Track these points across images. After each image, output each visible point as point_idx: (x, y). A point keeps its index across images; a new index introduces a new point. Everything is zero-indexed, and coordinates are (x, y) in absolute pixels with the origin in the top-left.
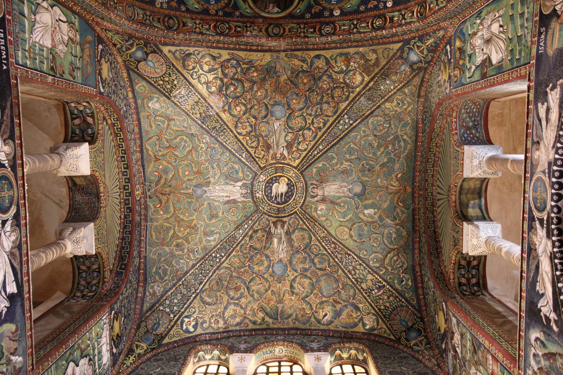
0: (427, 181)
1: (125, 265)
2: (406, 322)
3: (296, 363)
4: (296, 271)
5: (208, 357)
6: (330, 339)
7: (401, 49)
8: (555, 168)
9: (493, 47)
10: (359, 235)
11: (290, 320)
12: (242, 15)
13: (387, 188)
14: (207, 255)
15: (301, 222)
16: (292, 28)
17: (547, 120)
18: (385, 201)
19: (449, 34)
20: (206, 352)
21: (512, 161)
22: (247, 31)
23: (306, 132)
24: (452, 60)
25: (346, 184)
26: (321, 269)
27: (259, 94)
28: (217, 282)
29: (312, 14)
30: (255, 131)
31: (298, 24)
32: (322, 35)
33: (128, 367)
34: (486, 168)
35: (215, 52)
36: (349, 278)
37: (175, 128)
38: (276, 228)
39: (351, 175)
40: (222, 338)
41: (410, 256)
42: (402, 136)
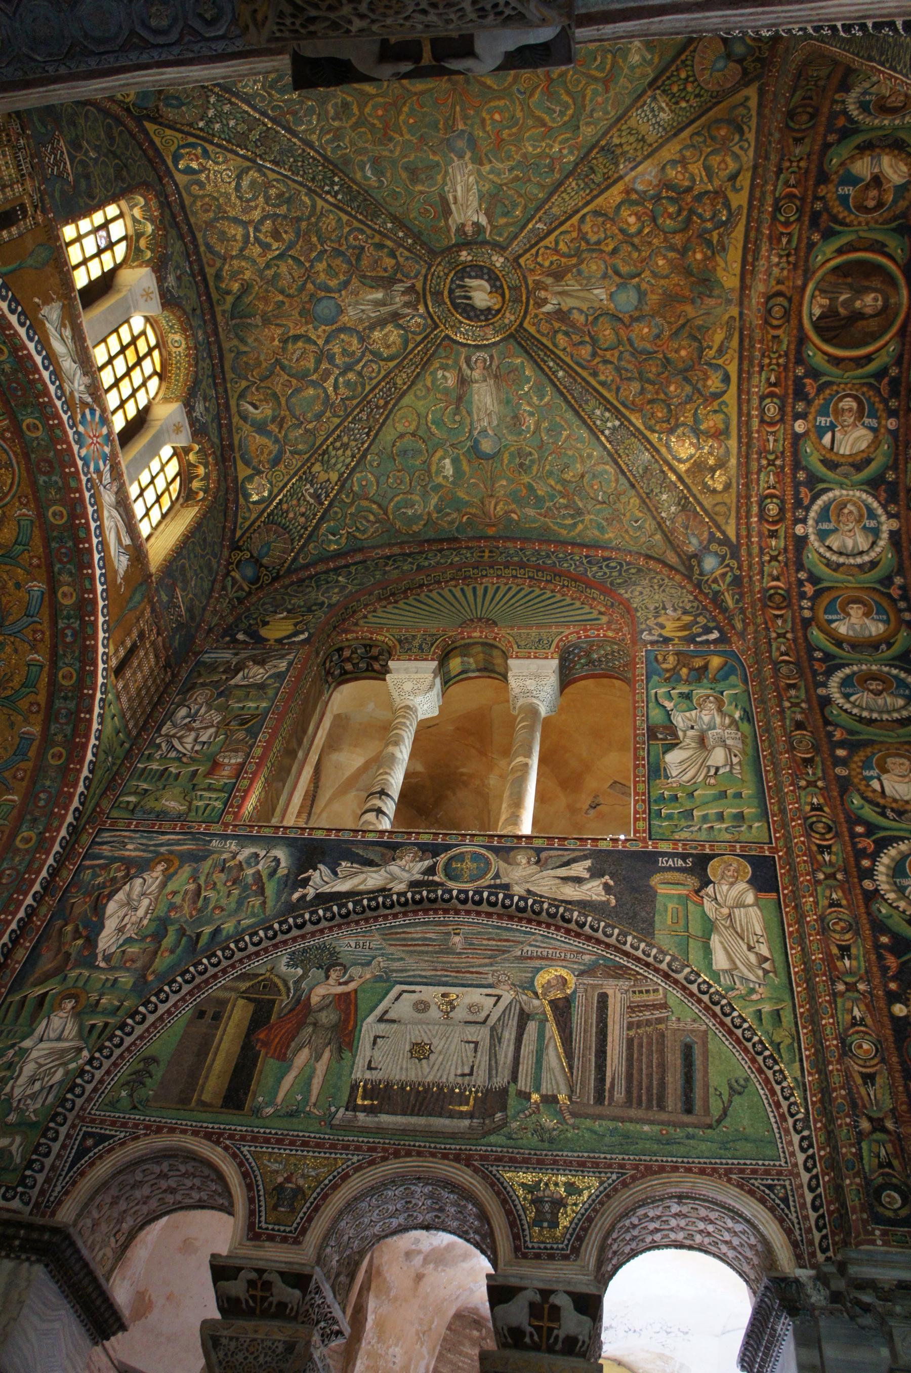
0: (506, 567)
2: (267, 554)
3: (161, 376)
4: (327, 342)
5: (137, 212)
7: (726, 541)
8: (501, 896)
9: (690, 752)
10: (405, 452)
11: (236, 342)
12: (811, 245)
15: (419, 338)
16: (780, 342)
17: (565, 879)
18: (468, 493)
19: (734, 639)
20: (146, 208)
21: (526, 765)
22: (780, 257)
23: (589, 348)
24: (692, 647)
25: (495, 423)
27: (661, 263)
29: (802, 378)
30: (590, 250)
31: (786, 354)
32: (762, 398)
34: (521, 702)
35: (745, 180)
36: (326, 439)
37: (589, 92)
38: (404, 293)
39: (511, 432)
40: (177, 225)
42: (582, 521)
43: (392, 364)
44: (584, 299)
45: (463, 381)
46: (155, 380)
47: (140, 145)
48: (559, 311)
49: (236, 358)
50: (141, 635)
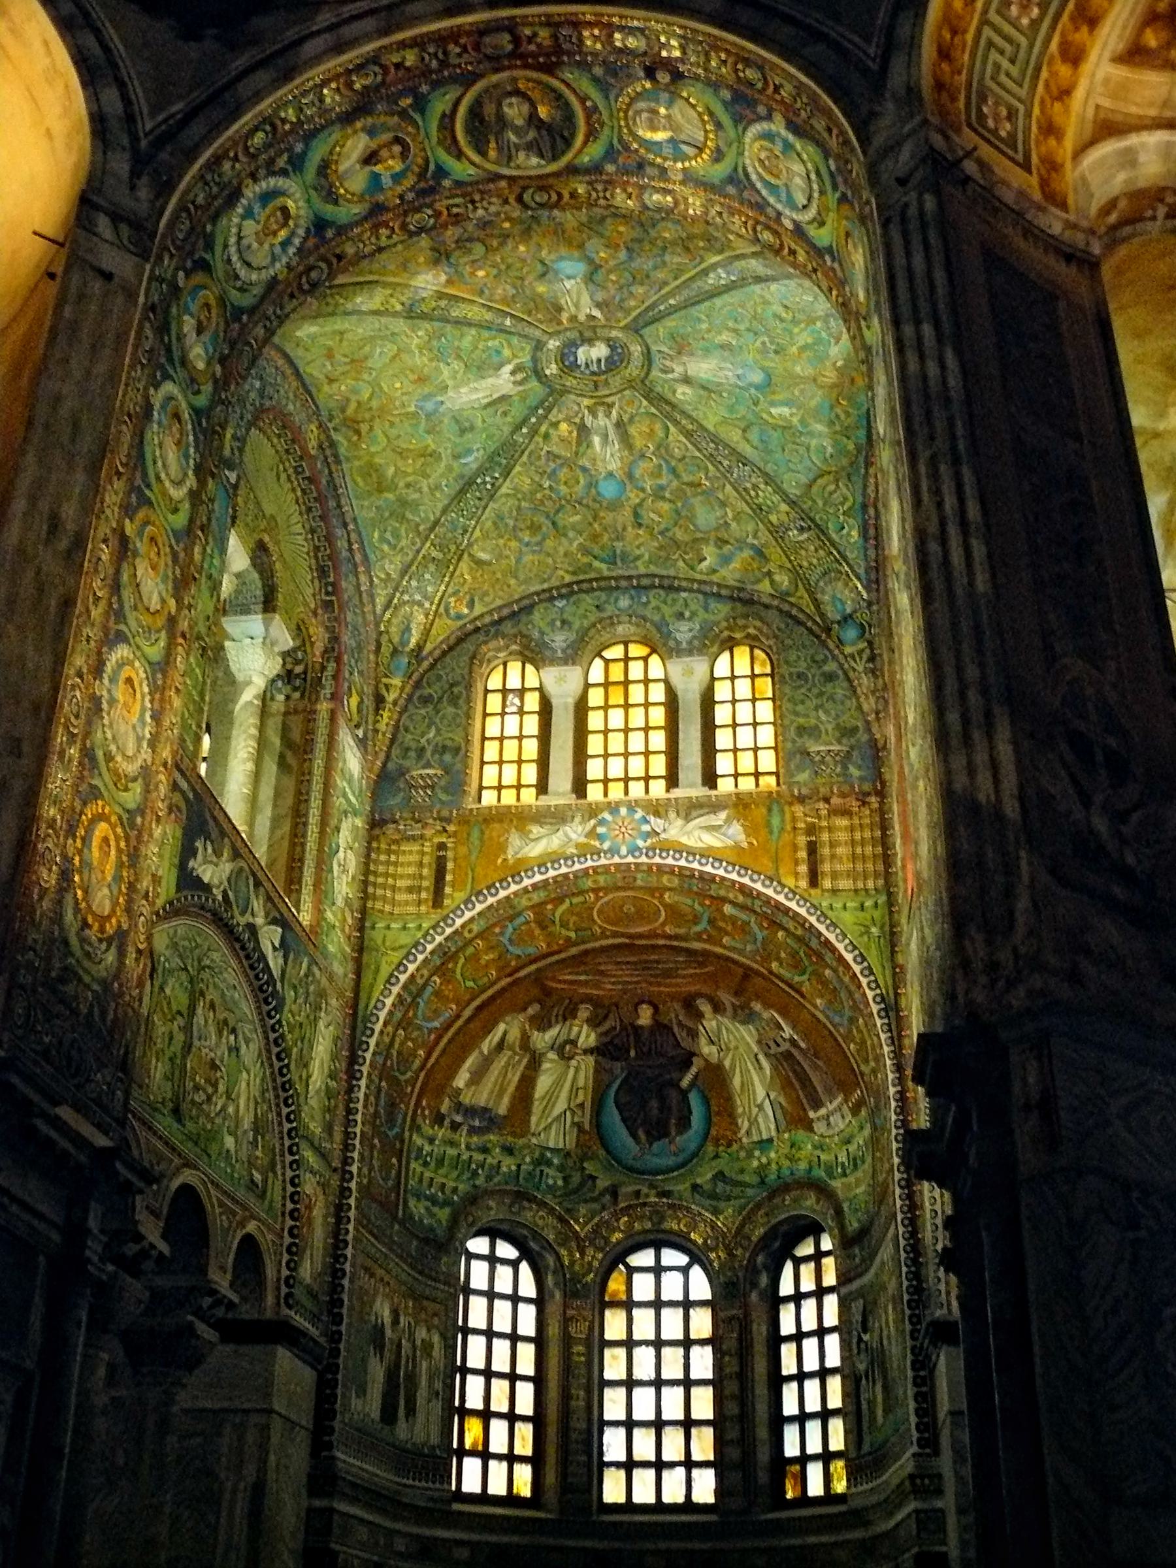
1: (333, 584)
2: (843, 603)
3: (654, 651)
5: (501, 655)
6: (713, 604)
11: (639, 563)
12: (458, 184)
13: (815, 380)
14: (468, 484)
15: (645, 403)
18: (812, 398)
20: (499, 650)
22: (476, 208)
26: (691, 484)
28: (495, 523)
31: (590, 183)
33: (384, 734)
38: (595, 416)
40: (521, 610)
41: (859, 486)
43: (672, 429)
44: (579, 294)
45: (687, 380)
46: (655, 660)
47: (444, 654)
48: (598, 305)
49: (656, 565)
50: (811, 830)
